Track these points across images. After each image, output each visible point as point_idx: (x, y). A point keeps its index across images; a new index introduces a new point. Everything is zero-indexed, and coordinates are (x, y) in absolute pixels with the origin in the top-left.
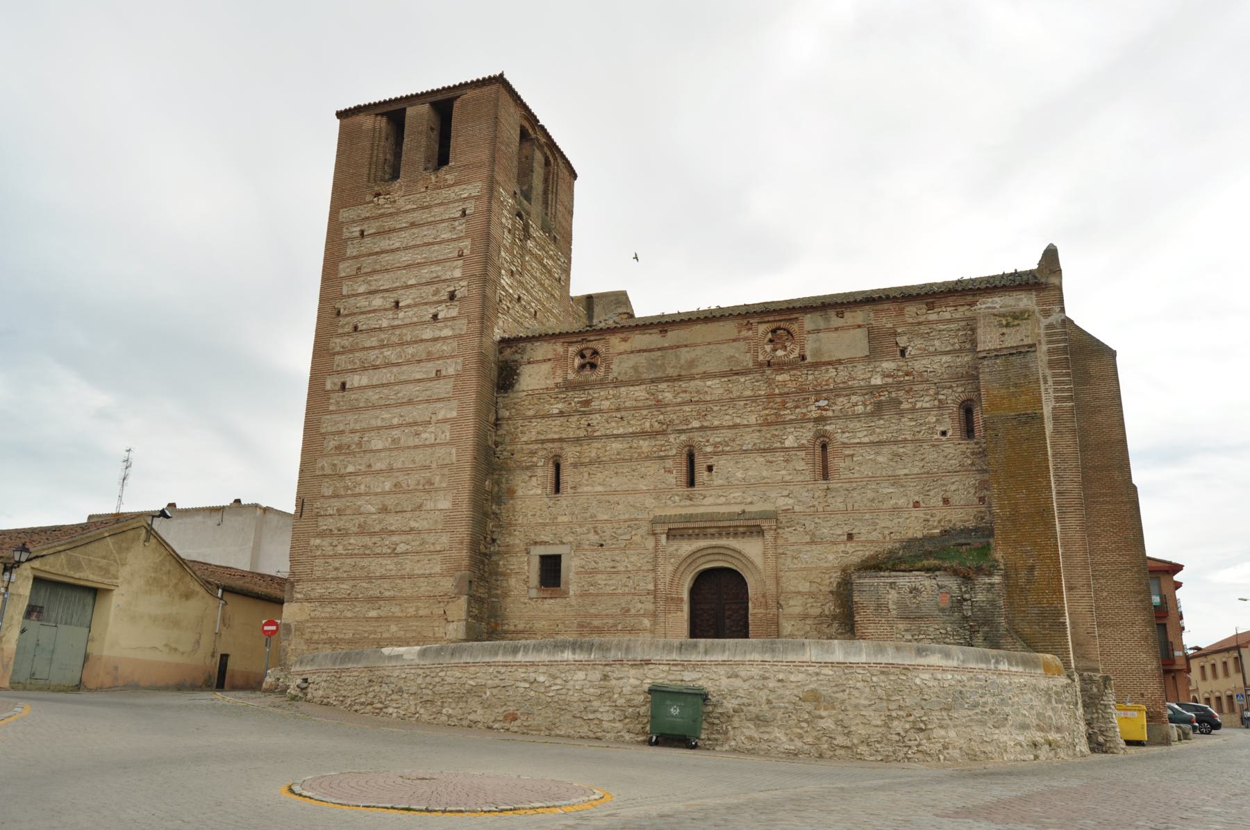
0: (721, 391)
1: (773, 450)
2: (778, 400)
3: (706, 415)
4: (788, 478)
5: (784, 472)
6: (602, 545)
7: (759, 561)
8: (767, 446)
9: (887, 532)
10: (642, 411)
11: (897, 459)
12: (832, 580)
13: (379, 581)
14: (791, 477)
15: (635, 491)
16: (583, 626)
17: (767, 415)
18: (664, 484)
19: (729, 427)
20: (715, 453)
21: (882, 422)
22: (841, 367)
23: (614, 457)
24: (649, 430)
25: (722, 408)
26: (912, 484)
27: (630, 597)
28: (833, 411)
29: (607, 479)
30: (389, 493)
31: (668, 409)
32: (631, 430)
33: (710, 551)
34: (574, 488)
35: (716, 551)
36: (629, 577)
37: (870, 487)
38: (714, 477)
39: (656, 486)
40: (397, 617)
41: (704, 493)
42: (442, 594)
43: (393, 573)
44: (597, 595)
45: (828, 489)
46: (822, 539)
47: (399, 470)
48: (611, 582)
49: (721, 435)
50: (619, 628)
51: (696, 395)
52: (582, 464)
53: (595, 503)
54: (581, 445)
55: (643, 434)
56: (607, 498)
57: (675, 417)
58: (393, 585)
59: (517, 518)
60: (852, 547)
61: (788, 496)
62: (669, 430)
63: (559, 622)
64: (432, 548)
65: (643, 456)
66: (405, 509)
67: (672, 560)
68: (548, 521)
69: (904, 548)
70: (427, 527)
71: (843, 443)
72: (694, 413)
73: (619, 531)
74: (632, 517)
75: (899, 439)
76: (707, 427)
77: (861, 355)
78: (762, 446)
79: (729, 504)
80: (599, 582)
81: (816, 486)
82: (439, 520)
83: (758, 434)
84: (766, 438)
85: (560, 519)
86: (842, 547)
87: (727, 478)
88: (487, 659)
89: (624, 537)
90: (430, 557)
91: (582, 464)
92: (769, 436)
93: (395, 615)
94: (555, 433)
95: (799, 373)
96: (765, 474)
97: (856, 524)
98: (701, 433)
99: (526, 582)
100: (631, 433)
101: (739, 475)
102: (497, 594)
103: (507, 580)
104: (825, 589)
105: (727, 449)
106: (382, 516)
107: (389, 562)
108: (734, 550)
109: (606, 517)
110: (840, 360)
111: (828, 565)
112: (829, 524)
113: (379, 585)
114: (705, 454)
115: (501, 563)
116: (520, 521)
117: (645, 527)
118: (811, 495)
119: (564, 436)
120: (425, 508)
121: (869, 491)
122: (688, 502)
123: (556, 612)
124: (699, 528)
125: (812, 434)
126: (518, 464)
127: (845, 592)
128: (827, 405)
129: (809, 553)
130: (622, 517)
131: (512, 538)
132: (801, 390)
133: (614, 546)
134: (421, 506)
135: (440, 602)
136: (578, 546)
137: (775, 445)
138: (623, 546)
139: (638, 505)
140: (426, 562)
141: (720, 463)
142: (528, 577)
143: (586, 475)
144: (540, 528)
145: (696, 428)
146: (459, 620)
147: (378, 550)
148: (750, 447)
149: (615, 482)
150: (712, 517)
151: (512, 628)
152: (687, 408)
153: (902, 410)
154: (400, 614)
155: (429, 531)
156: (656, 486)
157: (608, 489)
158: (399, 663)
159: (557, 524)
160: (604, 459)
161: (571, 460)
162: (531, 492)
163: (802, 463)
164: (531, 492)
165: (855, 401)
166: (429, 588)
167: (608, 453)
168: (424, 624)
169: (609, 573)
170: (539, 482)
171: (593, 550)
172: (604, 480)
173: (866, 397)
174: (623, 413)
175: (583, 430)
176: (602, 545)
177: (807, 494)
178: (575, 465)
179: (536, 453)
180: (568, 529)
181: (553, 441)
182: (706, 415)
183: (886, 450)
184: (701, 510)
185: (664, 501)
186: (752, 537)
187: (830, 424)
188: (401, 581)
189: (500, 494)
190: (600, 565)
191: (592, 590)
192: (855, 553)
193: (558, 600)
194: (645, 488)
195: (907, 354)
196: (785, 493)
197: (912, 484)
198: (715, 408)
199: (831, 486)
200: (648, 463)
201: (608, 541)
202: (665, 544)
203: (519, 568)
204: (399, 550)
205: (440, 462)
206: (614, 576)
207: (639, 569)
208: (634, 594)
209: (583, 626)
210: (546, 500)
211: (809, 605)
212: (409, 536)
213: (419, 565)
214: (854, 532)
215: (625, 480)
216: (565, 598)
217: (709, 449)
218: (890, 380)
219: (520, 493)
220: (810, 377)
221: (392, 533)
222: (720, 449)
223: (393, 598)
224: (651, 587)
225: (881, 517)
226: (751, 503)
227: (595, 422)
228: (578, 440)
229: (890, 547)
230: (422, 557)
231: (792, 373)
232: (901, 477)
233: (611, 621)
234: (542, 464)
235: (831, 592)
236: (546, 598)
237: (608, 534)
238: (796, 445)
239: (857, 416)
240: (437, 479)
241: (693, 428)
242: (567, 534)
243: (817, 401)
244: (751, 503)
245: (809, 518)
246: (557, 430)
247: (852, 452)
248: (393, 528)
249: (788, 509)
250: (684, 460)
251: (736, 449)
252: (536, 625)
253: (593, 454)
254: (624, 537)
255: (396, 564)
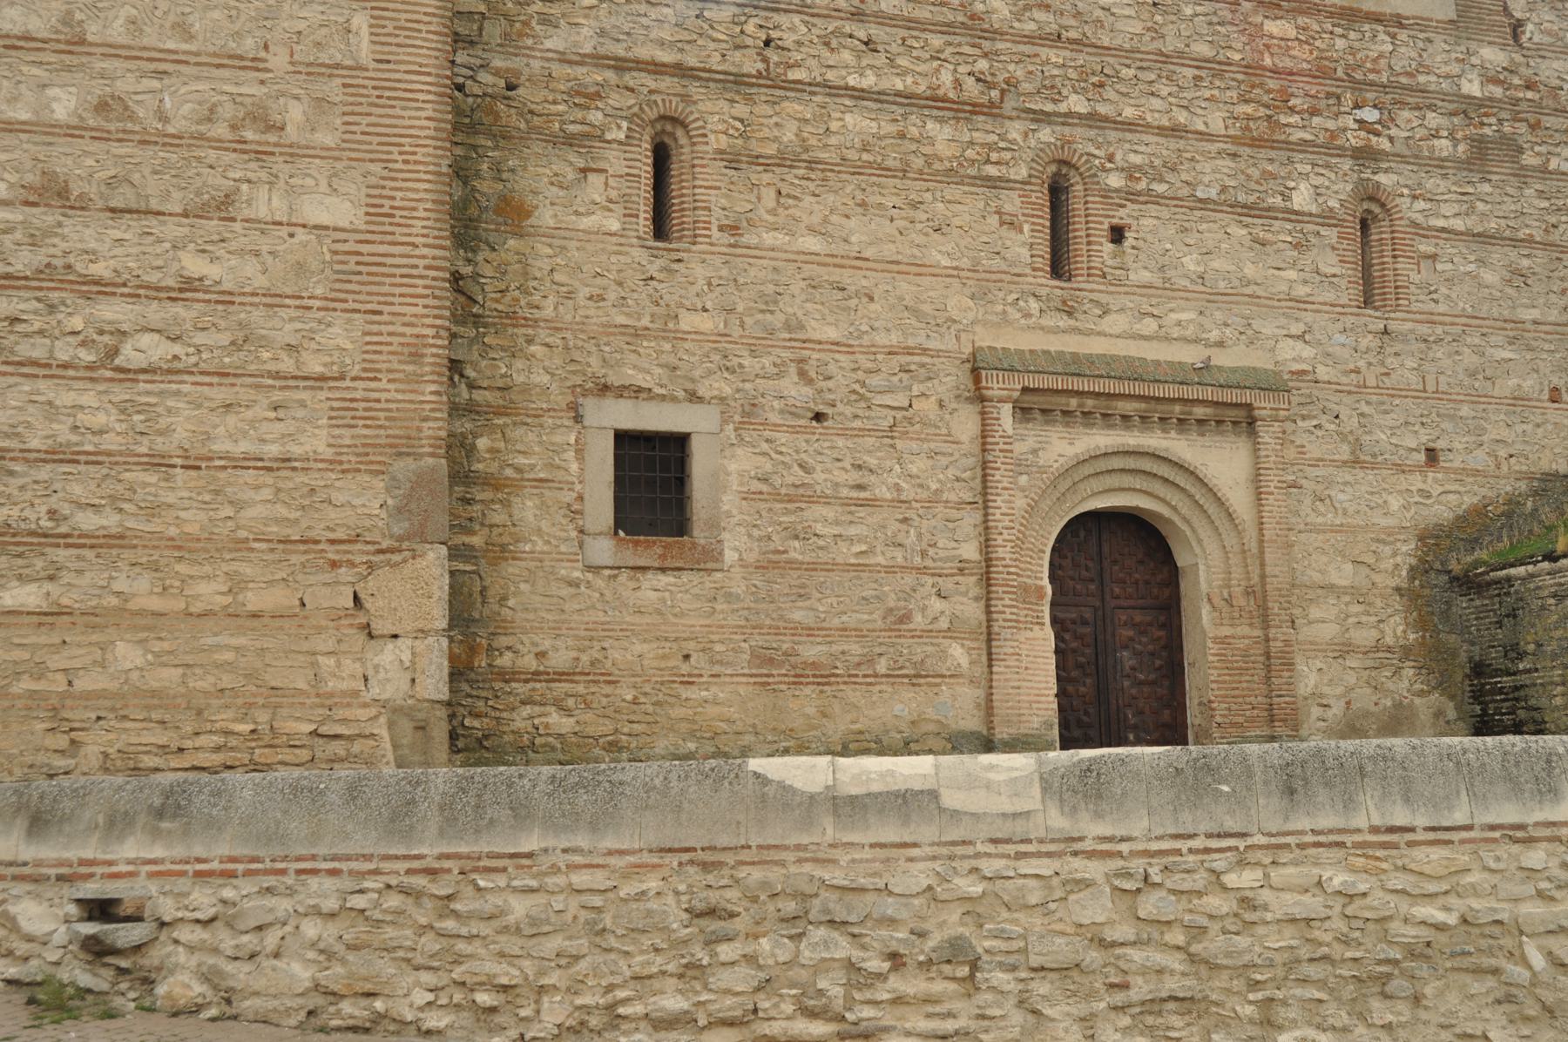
0: (1137, 28)
1: (1268, 213)
2: (1272, 84)
3: (1102, 85)
4: (1301, 291)
5: (1292, 274)
6: (818, 417)
7: (1239, 500)
8: (1251, 199)
9: (1502, 453)
10: (929, 36)
11: (1518, 281)
12: (1399, 559)
13: (44, 472)
14: (1308, 290)
15: (920, 269)
16: (771, 661)
17: (1249, 118)
18: (998, 260)
19: (1162, 131)
20: (1131, 196)
21: (1487, 188)
22: (1403, 35)
23: (852, 155)
24: (952, 95)
25: (1140, 75)
26: (1547, 346)
27: (909, 579)
28: (1391, 139)
29: (834, 218)
30: (72, 131)
31: (1000, 45)
32: (900, 86)
33: (1117, 463)
34: (733, 229)
35: (1131, 463)
36: (905, 520)
37: (1469, 340)
38: (1129, 260)
39: (976, 262)
40: (141, 613)
41: (1104, 298)
42: (340, 534)
43: (111, 442)
44: (812, 567)
45: (1386, 332)
46: (1374, 456)
47: (113, 51)
48: (853, 531)
49: (1142, 148)
50: (882, 666)
51: (1073, 22)
52: (755, 160)
53: (797, 286)
54: (749, 99)
55: (934, 102)
56: (837, 275)
57: (1020, 73)
58: (110, 487)
59: (536, 298)
60: (1436, 480)
61: (1301, 337)
62: (1009, 105)
63: (691, 645)
64: (287, 364)
65: (937, 166)
66: (154, 204)
67: (1023, 479)
68: (645, 322)
69: (1535, 493)
70: (261, 282)
71: (1415, 224)
72: (1072, 74)
73: (874, 381)
74: (911, 342)
75: (1521, 235)
76: (1106, 119)
77: (1441, 17)
78: (1242, 198)
79: (1168, 339)
80: (819, 528)
81: (1363, 320)
82: (314, 265)
83: (1229, 162)
84: (1249, 177)
85: (688, 321)
86: (1416, 482)
87: (1162, 269)
88: (1509, 813)
89: (888, 400)
90: (277, 396)
91: (755, 160)
92: (1255, 173)
93: (132, 605)
94: (662, 43)
95: (1316, 27)
96: (1249, 270)
97: (1443, 426)
98: (1093, 133)
99: (574, 513)
100: (898, 94)
101: (1191, 263)
102: (472, 547)
103: (506, 504)
104: (1387, 582)
105: (1160, 188)
106: (43, 217)
107: (88, 399)
108: (1179, 466)
109: (832, 333)
110: (1398, 16)
111: (1391, 522)
112: (1389, 420)
113: (47, 483)
114: (1106, 193)
115: (482, 443)
116: (548, 312)
117: (953, 378)
118: (1350, 341)
119: (692, 61)
120: (246, 213)
121: (1466, 349)
122: (1064, 322)
123: (682, 614)
124: (1098, 395)
125: (1349, 187)
126: (537, 121)
127: (1427, 592)
128: (1379, 122)
129: (1349, 489)
130: (881, 339)
131: (519, 364)
132: (1322, 72)
133: (857, 424)
134: (228, 200)
135: (334, 565)
136: (749, 415)
137: (1271, 200)
138: (885, 424)
139: (927, 308)
140: (260, 411)
141: (1145, 224)
142: (581, 498)
143: (769, 196)
144: (620, 341)
145: (1080, 116)
146: (423, 633)
147: (36, 349)
148: (1213, 193)
149: (859, 232)
150: (1133, 371)
151: (529, 663)
152: (1055, 55)
153: (1523, 168)
154: (156, 604)
155: (273, 299)
156: (976, 262)
157: (835, 249)
158: (926, 833)
159: (679, 337)
160: (823, 155)
161: (718, 141)
162: (586, 222)
163: (1332, 258)
164: (586, 222)
165: (1433, 125)
166: (282, 511)
167: (833, 140)
168: (268, 643)
169: (847, 503)
170: (613, 194)
171: (794, 430)
172: (825, 220)
173: (1455, 120)
174: (876, 32)
175: (752, 52)
176: (818, 417)
177: (1342, 339)
178: (732, 160)
179: (598, 95)
180: (716, 357)
181: (656, 68)
182: (1102, 85)
183: (1497, 255)
184: (1096, 346)
185: (999, 308)
186: (1222, 433)
187: (1386, 171)
188: (152, 478)
189: (473, 211)
190: (819, 476)
191: (796, 550)
192: (1443, 497)
193: (686, 577)
194: (945, 262)
195: (1524, 38)
196: (1296, 329)
197: (1547, 346)
198: (1125, 72)
199: (1392, 326)
200: (952, 192)
201: (840, 407)
202: (1010, 432)
203: (551, 466)
204: (129, 355)
205: (304, 53)
206: (862, 512)
207: (935, 499)
208: (922, 570)
209: (771, 661)
210: (639, 255)
211: (1351, 620)
212: (178, 309)
213: (231, 420)
214: (1440, 444)
215: (890, 229)
216: (710, 571)
217: (1115, 181)
218: (1498, 91)
219: (545, 217)
220: (1340, 44)
221: (99, 288)
222: (1142, 185)
223: (117, 540)
224: (970, 551)
225: (1493, 418)
226: (1220, 344)
227: (789, 39)
228: (738, 81)
229: (1509, 488)
230: (245, 394)
231: (1301, 20)
232: (1528, 326)
233: (855, 649)
234: (622, 136)
235: (1398, 589)
236: (644, 569)
237: (842, 381)
238: (1314, 209)
239: (1439, 164)
240: (295, 113)
241: (1070, 114)
242: (710, 373)
243: (1357, 106)
244: (1220, 344)
245: (1347, 400)
246: (666, 36)
247: (1430, 249)
248: (100, 269)
249: (1304, 372)
250: (1041, 197)
251: (1180, 194)
252: (615, 654)
253: (789, 136)
254: (888, 400)
255: (123, 410)
